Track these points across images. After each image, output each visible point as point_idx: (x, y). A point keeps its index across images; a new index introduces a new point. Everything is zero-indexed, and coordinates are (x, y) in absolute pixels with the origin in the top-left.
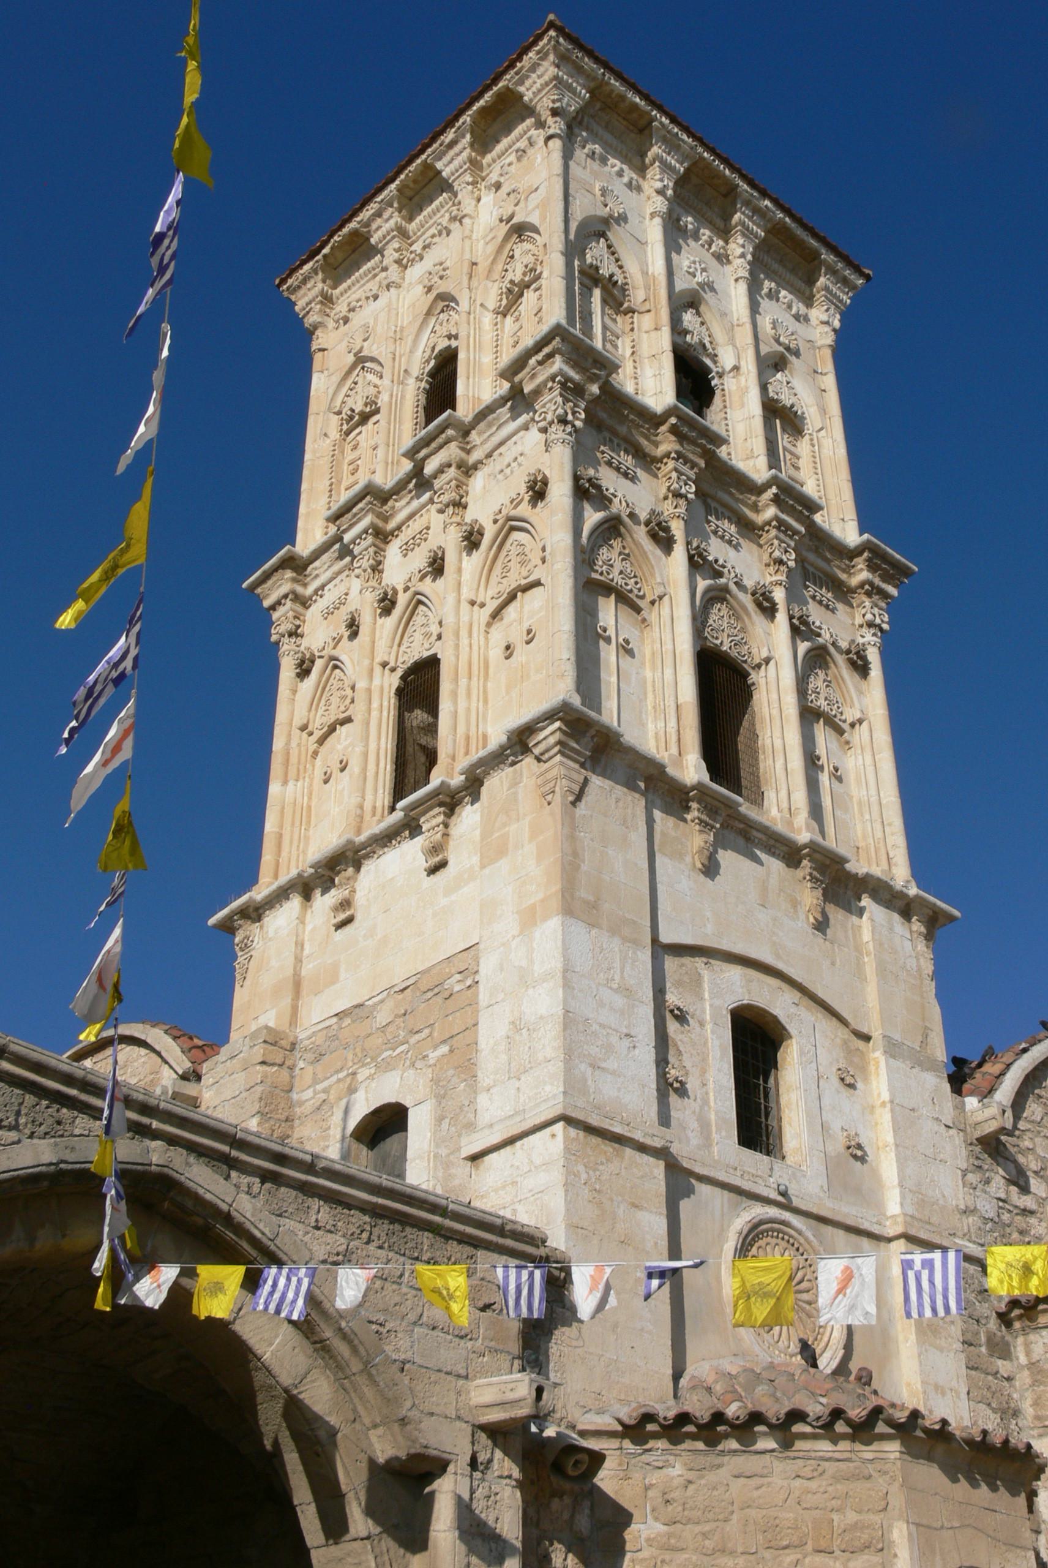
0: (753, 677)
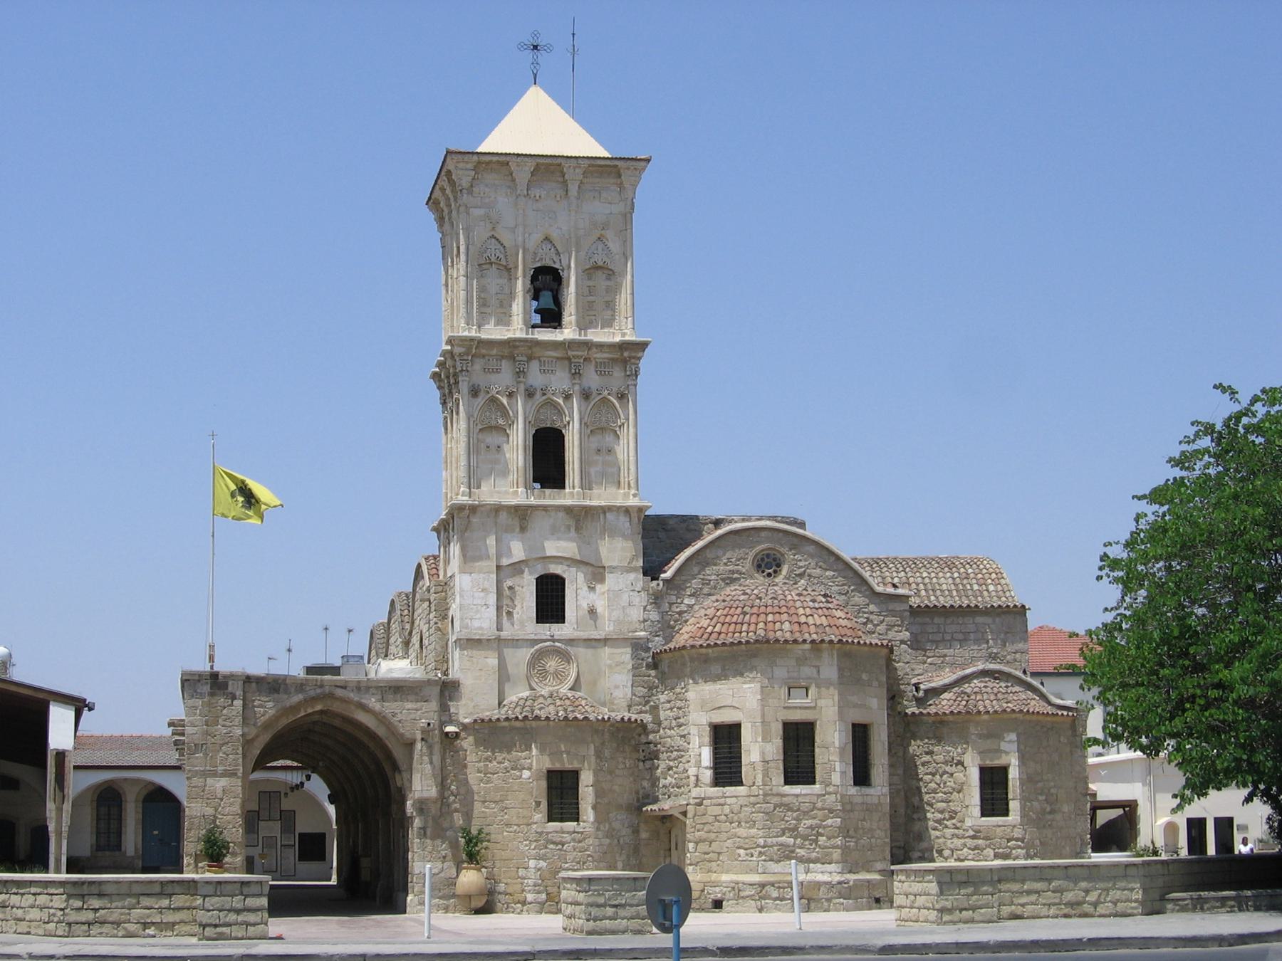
0: (563, 431)
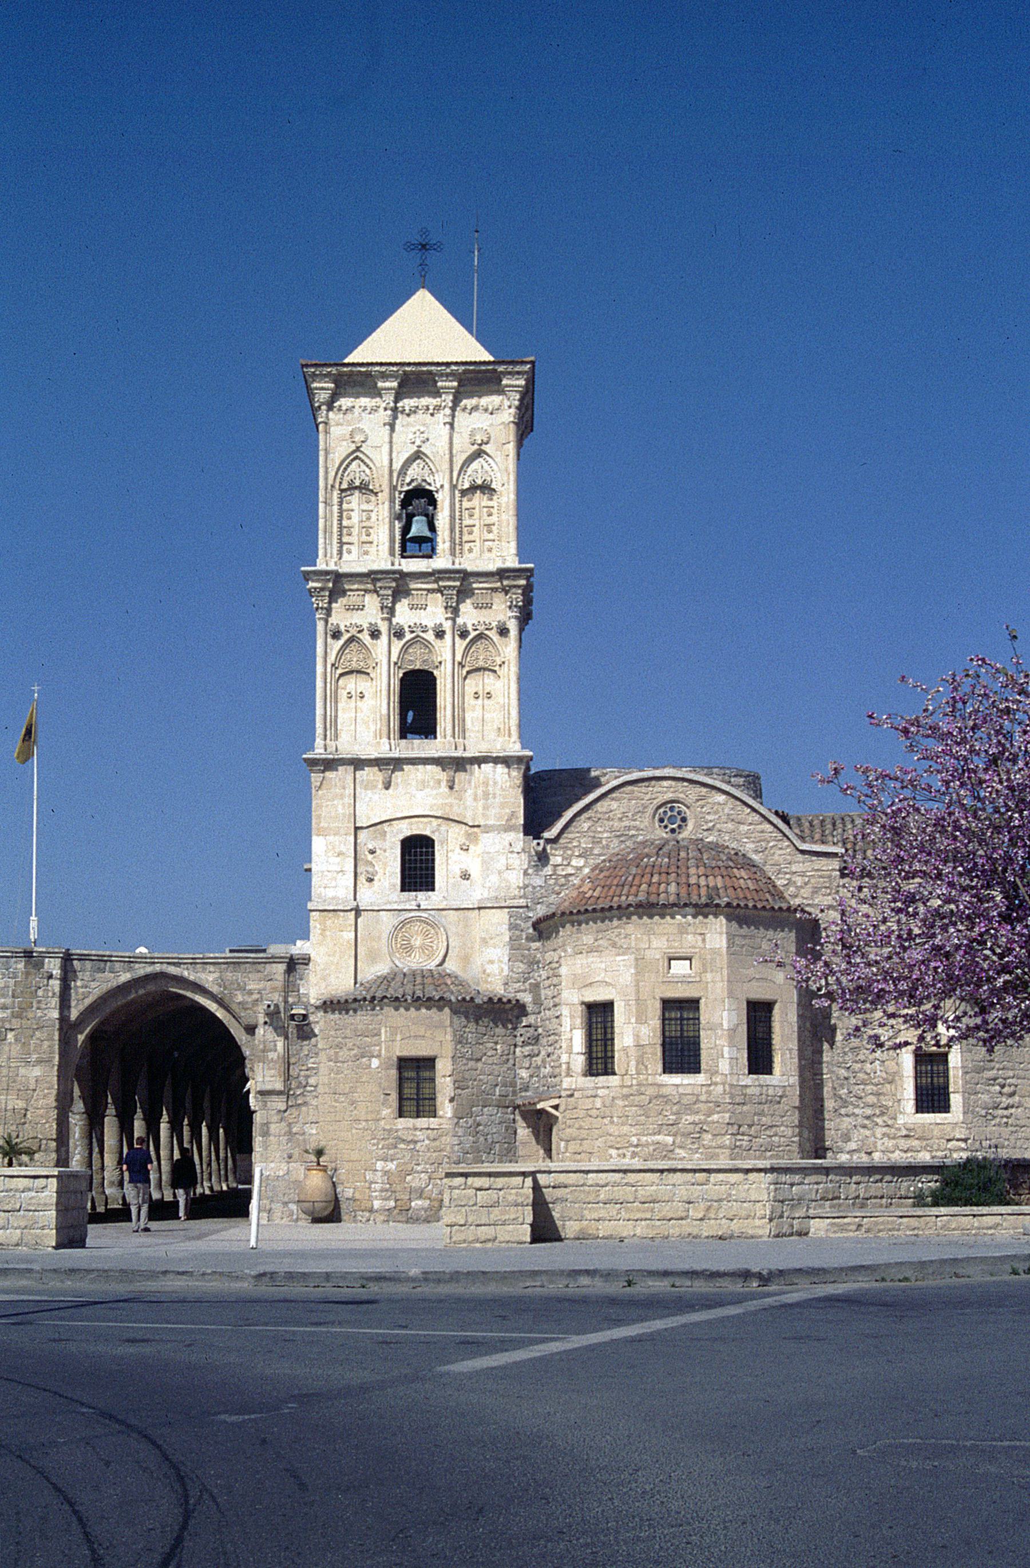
0: (435, 672)
